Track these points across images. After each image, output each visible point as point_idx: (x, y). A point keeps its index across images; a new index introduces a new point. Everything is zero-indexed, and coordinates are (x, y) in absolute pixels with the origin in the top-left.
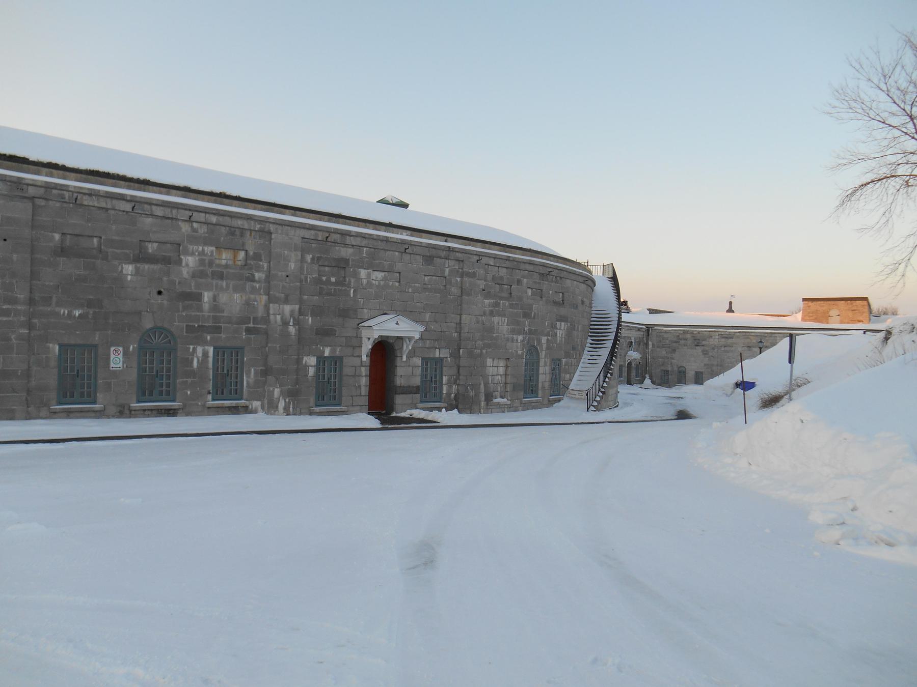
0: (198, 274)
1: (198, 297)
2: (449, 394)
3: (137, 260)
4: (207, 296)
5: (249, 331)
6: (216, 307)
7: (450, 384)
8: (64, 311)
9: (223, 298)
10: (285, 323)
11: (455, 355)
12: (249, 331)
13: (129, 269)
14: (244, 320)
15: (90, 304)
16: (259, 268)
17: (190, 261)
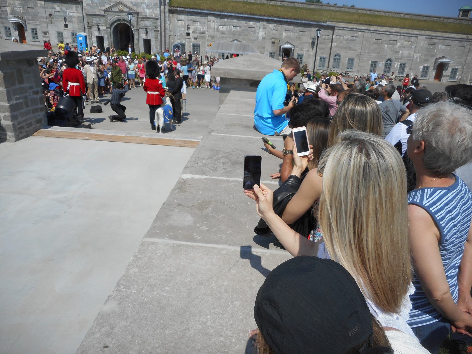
0: (400, 47)
1: (399, 52)
2: (458, 78)
3: (388, 44)
4: (401, 52)
5: (408, 60)
6: (402, 54)
7: (459, 76)
8: (373, 55)
9: (404, 52)
10: (417, 58)
11: (463, 68)
12: (408, 60)
13: (386, 46)
14: (408, 57)
15: (378, 53)
16: (413, 45)
17: (399, 44)
